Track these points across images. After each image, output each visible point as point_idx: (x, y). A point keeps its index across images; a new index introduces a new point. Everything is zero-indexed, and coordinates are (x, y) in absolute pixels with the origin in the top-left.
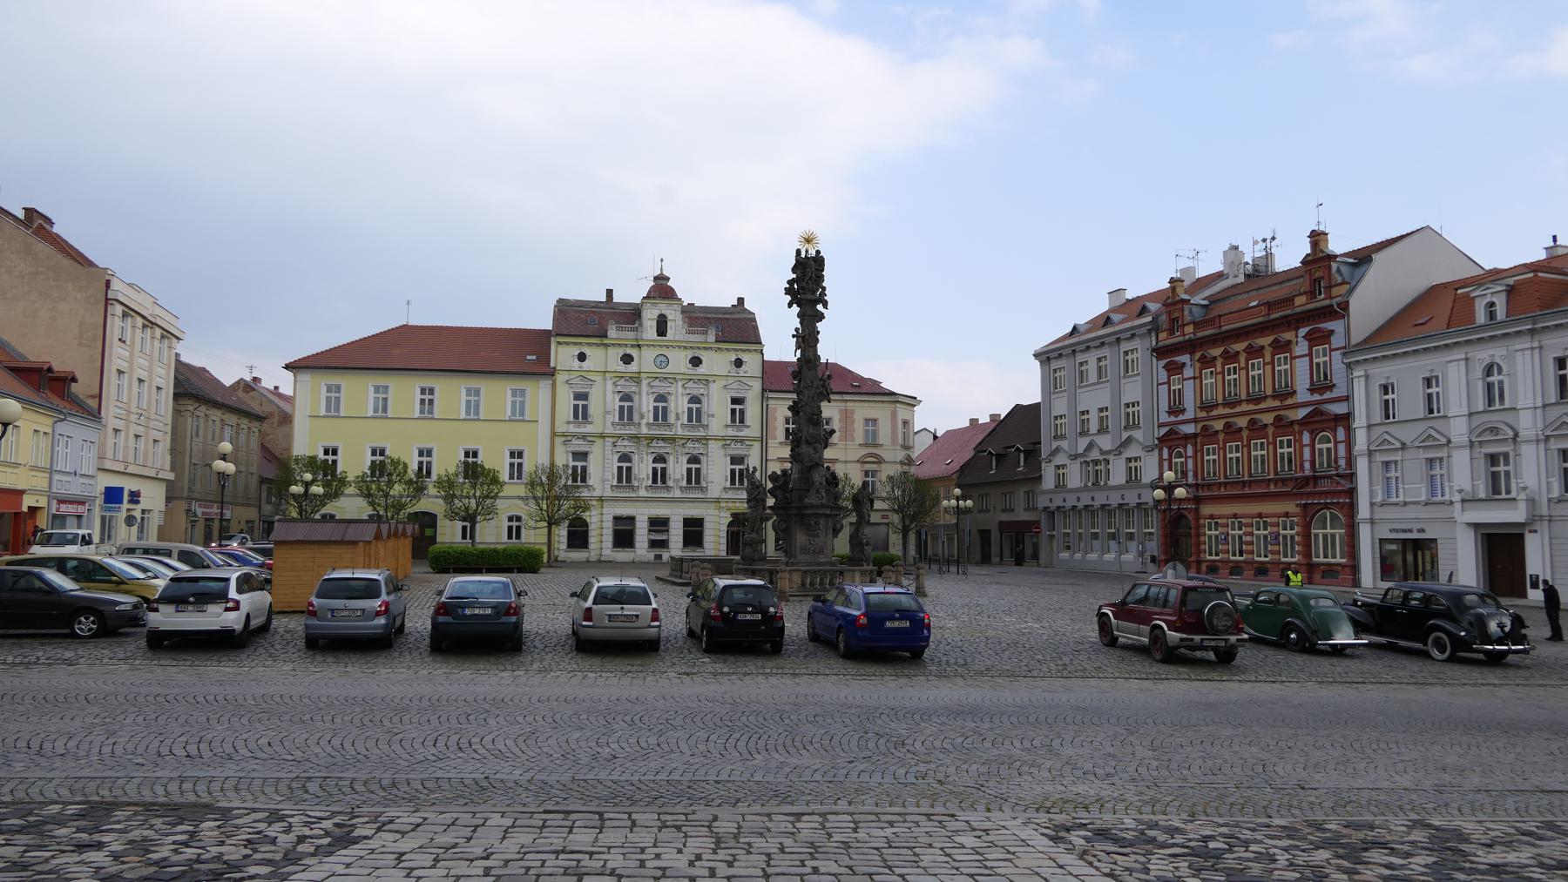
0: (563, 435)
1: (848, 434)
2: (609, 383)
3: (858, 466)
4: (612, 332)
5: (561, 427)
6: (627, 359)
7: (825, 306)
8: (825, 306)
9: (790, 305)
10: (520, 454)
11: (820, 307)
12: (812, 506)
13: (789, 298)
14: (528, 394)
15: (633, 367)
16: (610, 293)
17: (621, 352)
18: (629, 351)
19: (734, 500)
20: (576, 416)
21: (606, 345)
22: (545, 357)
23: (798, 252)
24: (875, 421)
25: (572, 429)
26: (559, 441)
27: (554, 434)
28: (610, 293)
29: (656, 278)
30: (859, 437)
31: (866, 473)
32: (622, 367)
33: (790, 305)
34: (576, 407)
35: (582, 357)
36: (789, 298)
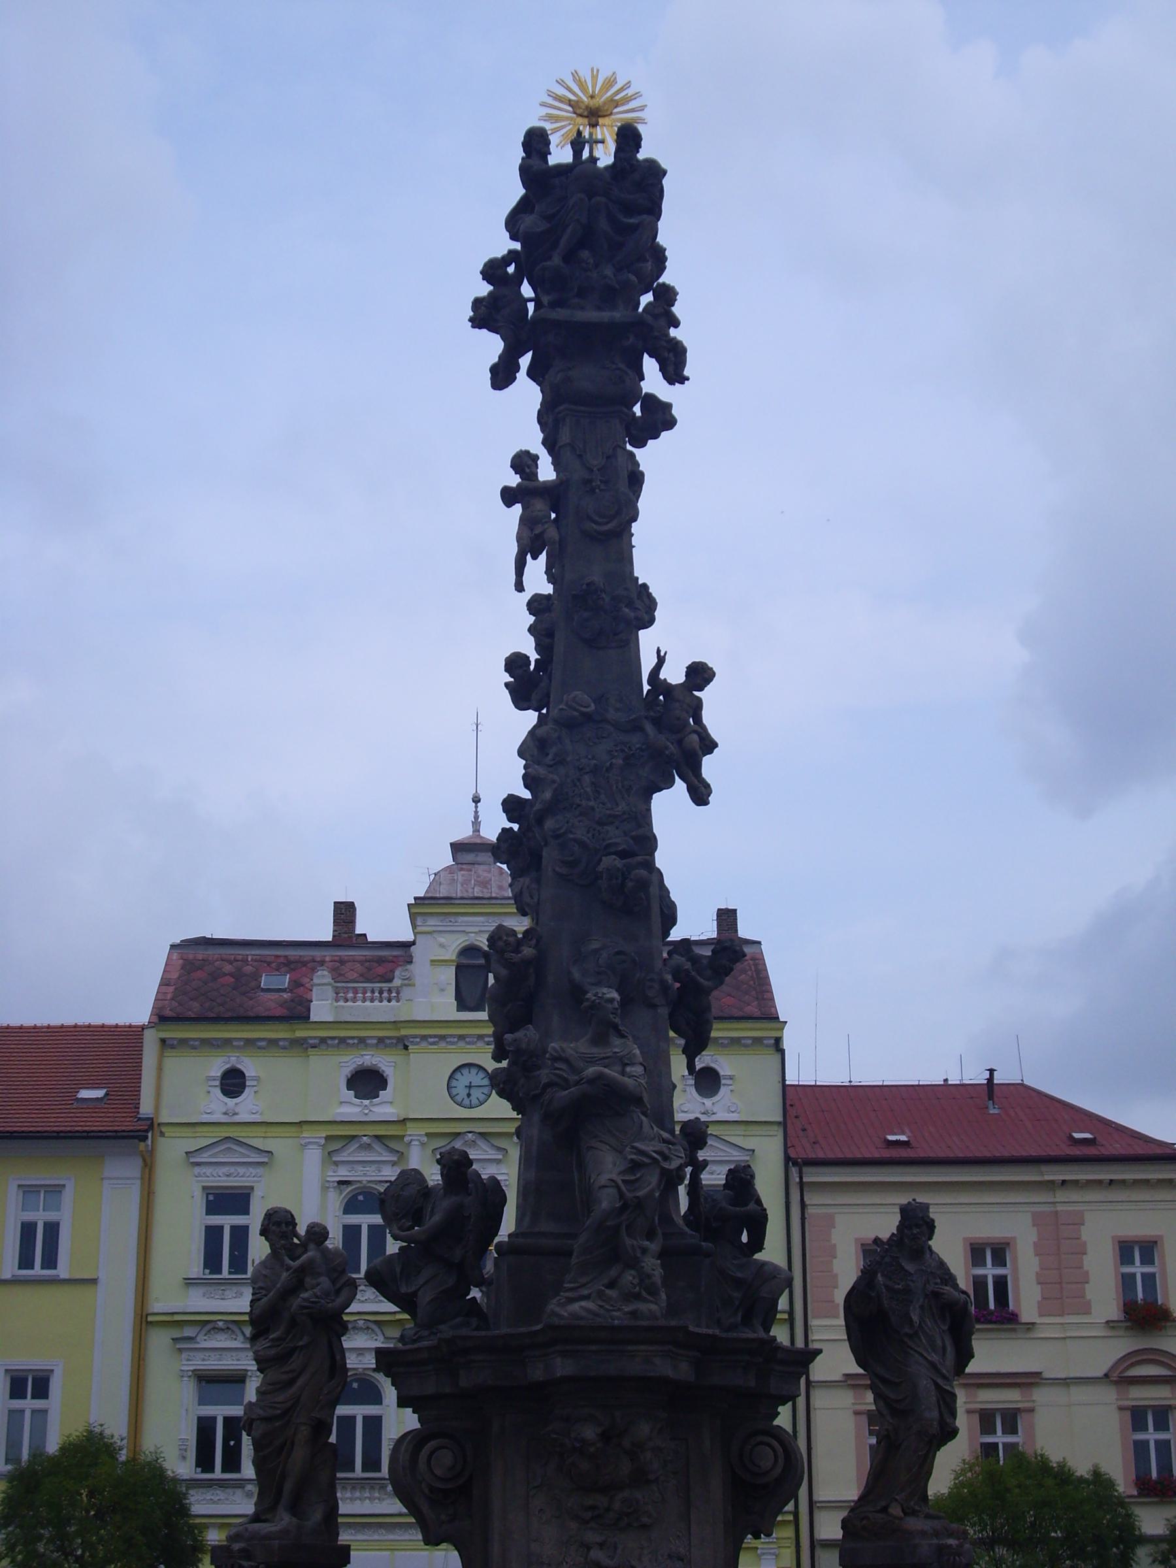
0: (173, 1322)
1: (1064, 1292)
2: (314, 1156)
3: (1109, 1395)
4: (322, 1008)
5: (168, 1298)
6: (367, 1082)
7: (674, 373)
8: (674, 373)
9: (502, 376)
10: (42, 1387)
11: (653, 380)
12: (569, 1336)
13: (492, 345)
14: (68, 1197)
15: (384, 1108)
16: (345, 913)
17: (352, 1061)
18: (369, 1058)
19: (208, 1324)
20: (212, 1261)
21: (301, 1046)
22: (126, 1086)
23: (535, 142)
24: (1149, 1249)
25: (200, 1302)
26: (159, 1341)
27: (144, 1322)
28: (345, 913)
29: (458, 848)
30: (1104, 1300)
31: (1137, 1417)
32: (351, 1108)
33: (502, 376)
34: (213, 1235)
35: (233, 1083)
36: (492, 345)
